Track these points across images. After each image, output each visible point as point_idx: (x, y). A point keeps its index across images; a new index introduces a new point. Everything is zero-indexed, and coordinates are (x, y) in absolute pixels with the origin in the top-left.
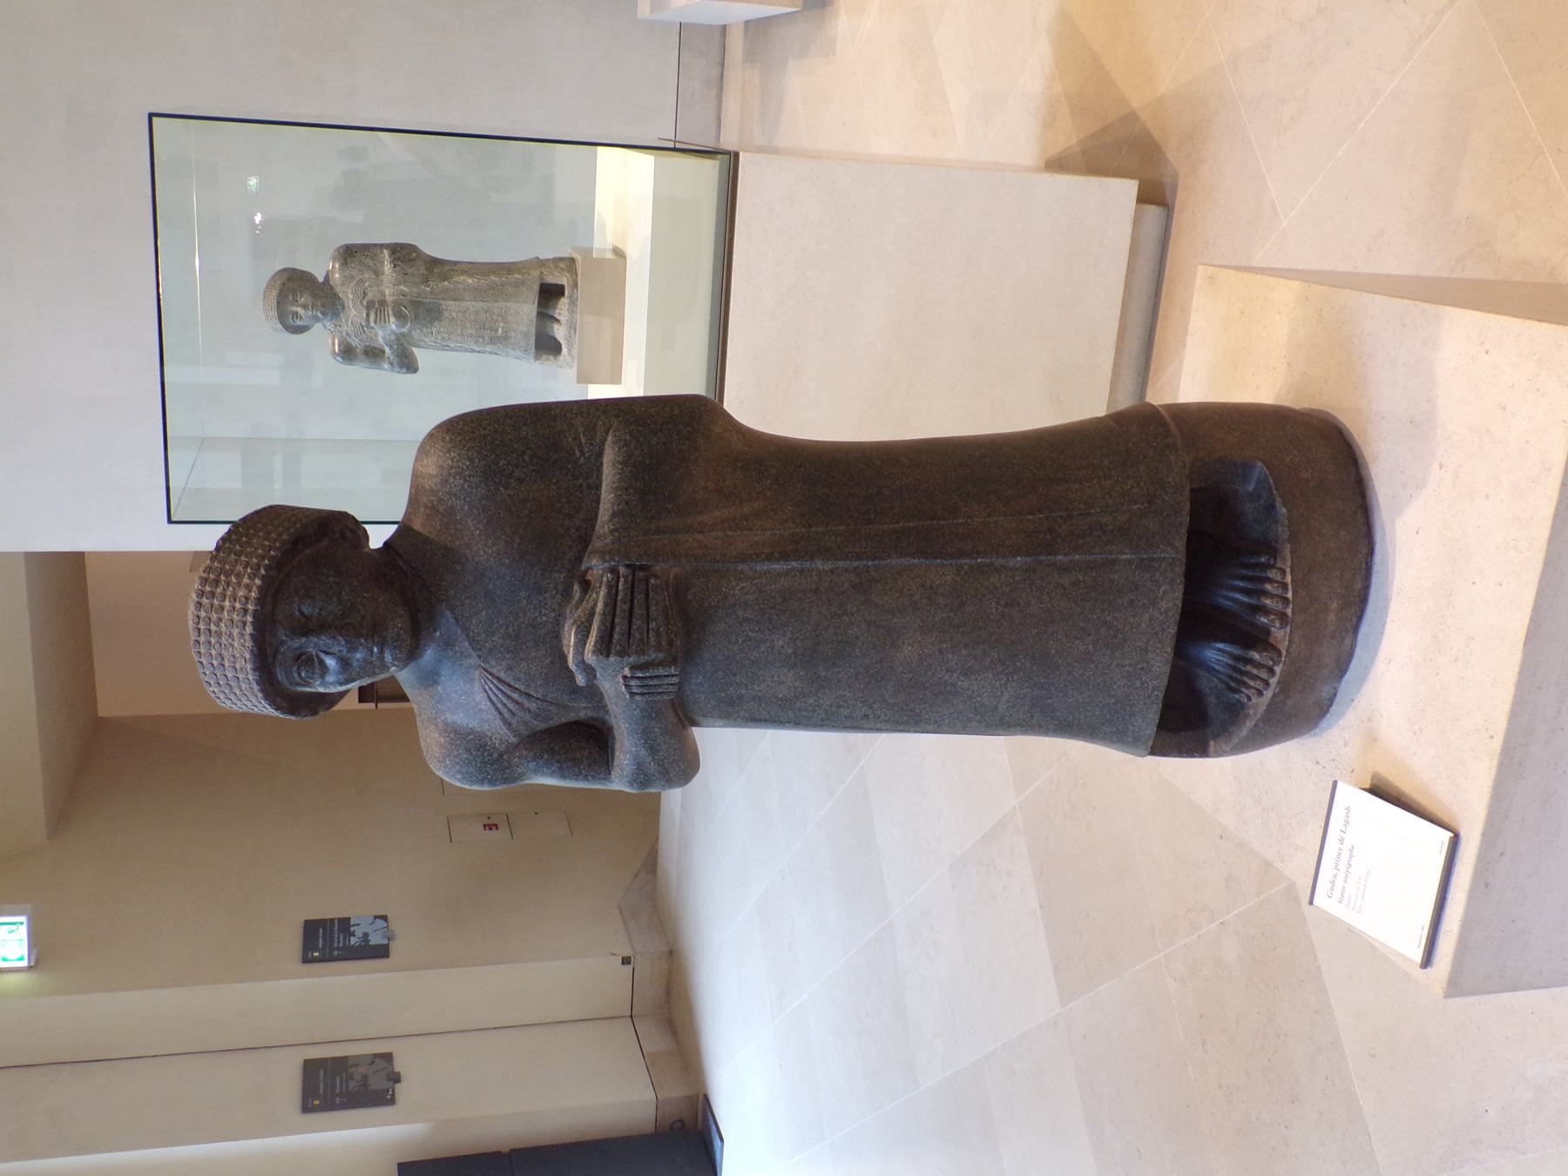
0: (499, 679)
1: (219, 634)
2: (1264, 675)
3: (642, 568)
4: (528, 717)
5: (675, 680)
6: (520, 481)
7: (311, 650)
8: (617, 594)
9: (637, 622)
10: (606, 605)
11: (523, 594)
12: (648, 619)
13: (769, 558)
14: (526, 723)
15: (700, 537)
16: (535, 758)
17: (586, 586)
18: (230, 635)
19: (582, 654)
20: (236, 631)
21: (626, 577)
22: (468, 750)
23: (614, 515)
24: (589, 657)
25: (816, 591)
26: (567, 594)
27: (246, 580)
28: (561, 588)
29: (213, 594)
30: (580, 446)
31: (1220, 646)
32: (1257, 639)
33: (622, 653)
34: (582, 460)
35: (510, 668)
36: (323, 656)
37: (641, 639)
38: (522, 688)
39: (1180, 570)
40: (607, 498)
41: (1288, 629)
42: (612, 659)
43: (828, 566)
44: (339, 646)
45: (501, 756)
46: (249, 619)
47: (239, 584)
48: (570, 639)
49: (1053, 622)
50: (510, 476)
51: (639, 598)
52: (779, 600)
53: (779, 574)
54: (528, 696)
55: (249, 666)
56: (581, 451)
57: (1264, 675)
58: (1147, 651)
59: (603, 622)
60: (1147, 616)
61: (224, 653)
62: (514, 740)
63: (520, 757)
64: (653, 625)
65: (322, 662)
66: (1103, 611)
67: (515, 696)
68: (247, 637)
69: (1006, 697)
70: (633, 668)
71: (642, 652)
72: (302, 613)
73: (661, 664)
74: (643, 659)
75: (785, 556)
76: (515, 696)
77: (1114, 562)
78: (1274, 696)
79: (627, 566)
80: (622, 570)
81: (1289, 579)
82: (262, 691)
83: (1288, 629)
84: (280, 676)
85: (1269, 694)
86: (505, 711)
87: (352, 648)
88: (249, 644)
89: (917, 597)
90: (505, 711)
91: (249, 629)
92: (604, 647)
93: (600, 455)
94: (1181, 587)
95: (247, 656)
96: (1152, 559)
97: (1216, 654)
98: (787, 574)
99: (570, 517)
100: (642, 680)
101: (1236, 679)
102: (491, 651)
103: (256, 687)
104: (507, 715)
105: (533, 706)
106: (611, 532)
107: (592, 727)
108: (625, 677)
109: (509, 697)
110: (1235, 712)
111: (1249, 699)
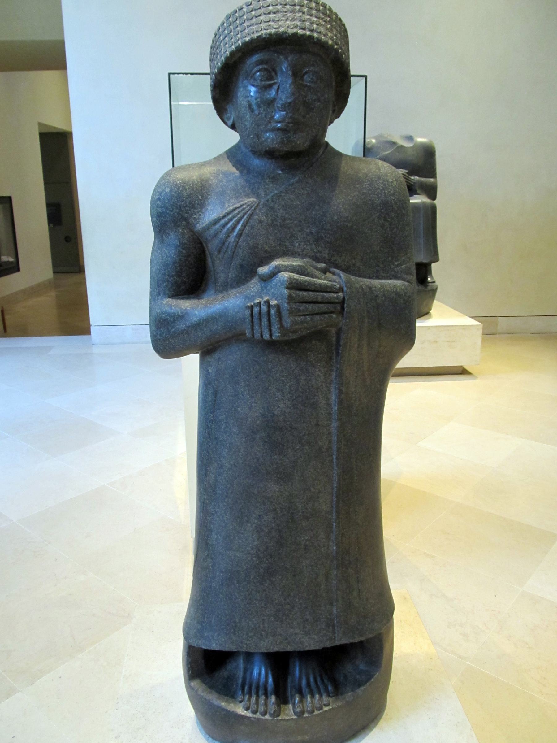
0: (251, 215)
1: (293, 11)
2: (262, 709)
3: (343, 308)
4: (222, 235)
5: (257, 335)
6: (383, 226)
7: (279, 79)
8: (326, 292)
9: (310, 307)
10: (320, 285)
11: (314, 230)
12: (312, 314)
13: (341, 392)
14: (216, 235)
15: (356, 345)
16: (182, 244)
17: (325, 271)
18: (293, 19)
19: (285, 271)
20: (299, 23)
21: (337, 298)
22: (189, 196)
23: (370, 288)
24: (285, 275)
25: (317, 425)
26: (317, 259)
27: (330, 34)
28: (318, 255)
29: (318, 11)
30: (401, 265)
31: (270, 676)
32: (283, 699)
33: (290, 299)
34: (393, 266)
35: (260, 222)
36: (276, 87)
37: (299, 311)
38: (246, 231)
39: (328, 645)
40: (377, 283)
41: (295, 717)
42: (286, 291)
43: (334, 431)
44: (284, 97)
45: (186, 219)
46: (308, 33)
47: (327, 29)
48: (295, 262)
49: (294, 576)
50: (385, 220)
51: (324, 307)
52: (312, 401)
53: (328, 399)
54: (240, 235)
55: (273, 31)
56: (397, 266)
57: (262, 709)
58: (274, 635)
59: (310, 284)
60: (297, 631)
61: (280, 15)
62: (199, 227)
63: (183, 233)
64: (308, 318)
65: (270, 86)
66: (301, 604)
67: (239, 226)
68: (295, 30)
69: (237, 554)
70: (278, 307)
71: (291, 312)
72: (306, 73)
73: (282, 326)
74: (285, 313)
75: (340, 402)
76: (239, 226)
77: (331, 604)
78: (249, 718)
79: (344, 298)
80: (341, 294)
81: (326, 709)
82: (252, 40)
83: (295, 717)
84: (255, 58)
85: (249, 714)
86: (226, 219)
87: (284, 108)
88: (291, 31)
89: (312, 490)
90: (226, 219)
91: (300, 32)
92: (294, 286)
93: (396, 278)
94: (317, 648)
95: (281, 30)
96: (333, 626)
97: (260, 672)
98: (329, 404)
99: (362, 259)
100: (255, 314)
101: (251, 689)
102: (272, 208)
103: (255, 36)
104: (223, 222)
105: (232, 239)
106: (361, 287)
107: (201, 283)
108: (267, 302)
109: (238, 222)
110: (227, 690)
111: (241, 702)
